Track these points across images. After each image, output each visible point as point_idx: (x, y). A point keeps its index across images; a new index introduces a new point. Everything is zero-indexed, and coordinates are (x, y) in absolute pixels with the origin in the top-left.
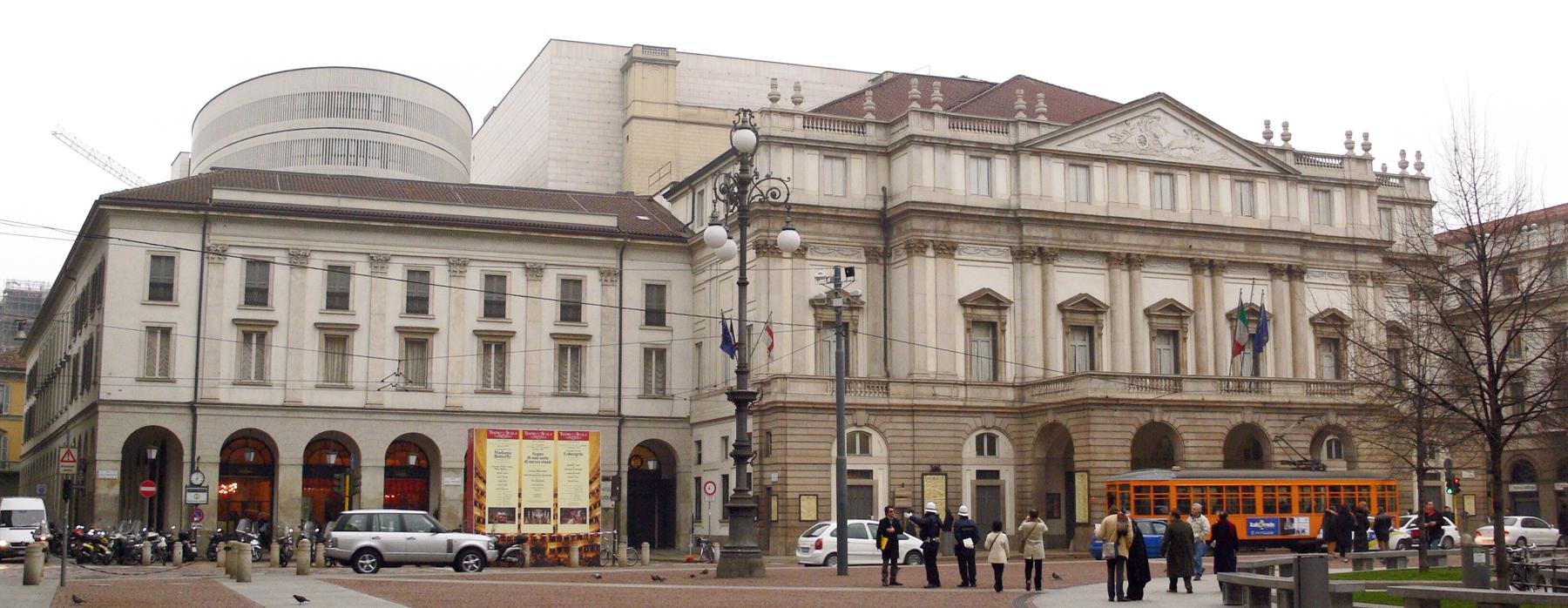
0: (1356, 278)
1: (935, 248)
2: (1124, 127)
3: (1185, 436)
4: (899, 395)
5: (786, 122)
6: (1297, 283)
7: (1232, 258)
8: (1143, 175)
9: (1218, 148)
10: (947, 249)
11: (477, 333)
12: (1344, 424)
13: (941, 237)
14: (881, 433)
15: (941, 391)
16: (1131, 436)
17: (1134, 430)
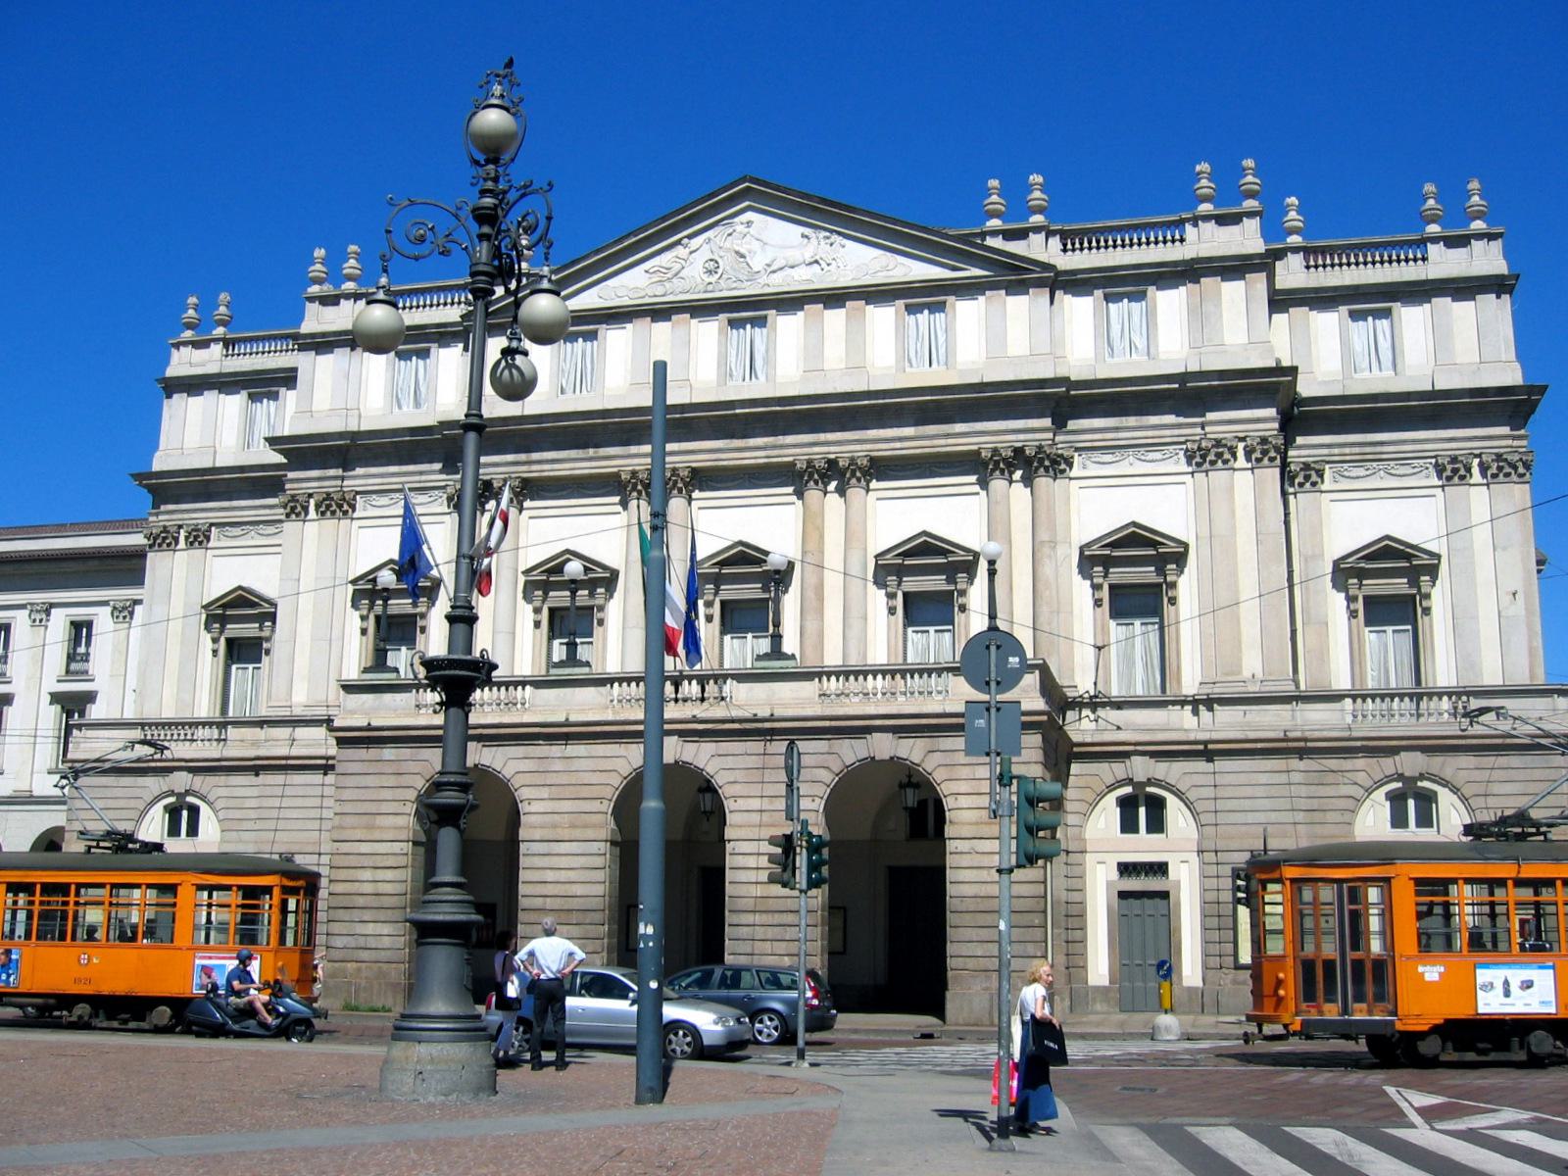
0: (1205, 457)
1: (318, 506)
2: (680, 251)
3: (523, 794)
4: (241, 744)
5: (199, 355)
6: (1042, 482)
7: (884, 450)
8: (707, 332)
9: (880, 252)
10: (337, 506)
11: (56, 698)
12: (916, 758)
13: (331, 486)
14: (210, 804)
15: (302, 732)
16: (412, 795)
17: (420, 783)
